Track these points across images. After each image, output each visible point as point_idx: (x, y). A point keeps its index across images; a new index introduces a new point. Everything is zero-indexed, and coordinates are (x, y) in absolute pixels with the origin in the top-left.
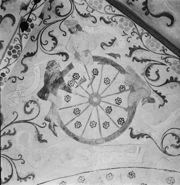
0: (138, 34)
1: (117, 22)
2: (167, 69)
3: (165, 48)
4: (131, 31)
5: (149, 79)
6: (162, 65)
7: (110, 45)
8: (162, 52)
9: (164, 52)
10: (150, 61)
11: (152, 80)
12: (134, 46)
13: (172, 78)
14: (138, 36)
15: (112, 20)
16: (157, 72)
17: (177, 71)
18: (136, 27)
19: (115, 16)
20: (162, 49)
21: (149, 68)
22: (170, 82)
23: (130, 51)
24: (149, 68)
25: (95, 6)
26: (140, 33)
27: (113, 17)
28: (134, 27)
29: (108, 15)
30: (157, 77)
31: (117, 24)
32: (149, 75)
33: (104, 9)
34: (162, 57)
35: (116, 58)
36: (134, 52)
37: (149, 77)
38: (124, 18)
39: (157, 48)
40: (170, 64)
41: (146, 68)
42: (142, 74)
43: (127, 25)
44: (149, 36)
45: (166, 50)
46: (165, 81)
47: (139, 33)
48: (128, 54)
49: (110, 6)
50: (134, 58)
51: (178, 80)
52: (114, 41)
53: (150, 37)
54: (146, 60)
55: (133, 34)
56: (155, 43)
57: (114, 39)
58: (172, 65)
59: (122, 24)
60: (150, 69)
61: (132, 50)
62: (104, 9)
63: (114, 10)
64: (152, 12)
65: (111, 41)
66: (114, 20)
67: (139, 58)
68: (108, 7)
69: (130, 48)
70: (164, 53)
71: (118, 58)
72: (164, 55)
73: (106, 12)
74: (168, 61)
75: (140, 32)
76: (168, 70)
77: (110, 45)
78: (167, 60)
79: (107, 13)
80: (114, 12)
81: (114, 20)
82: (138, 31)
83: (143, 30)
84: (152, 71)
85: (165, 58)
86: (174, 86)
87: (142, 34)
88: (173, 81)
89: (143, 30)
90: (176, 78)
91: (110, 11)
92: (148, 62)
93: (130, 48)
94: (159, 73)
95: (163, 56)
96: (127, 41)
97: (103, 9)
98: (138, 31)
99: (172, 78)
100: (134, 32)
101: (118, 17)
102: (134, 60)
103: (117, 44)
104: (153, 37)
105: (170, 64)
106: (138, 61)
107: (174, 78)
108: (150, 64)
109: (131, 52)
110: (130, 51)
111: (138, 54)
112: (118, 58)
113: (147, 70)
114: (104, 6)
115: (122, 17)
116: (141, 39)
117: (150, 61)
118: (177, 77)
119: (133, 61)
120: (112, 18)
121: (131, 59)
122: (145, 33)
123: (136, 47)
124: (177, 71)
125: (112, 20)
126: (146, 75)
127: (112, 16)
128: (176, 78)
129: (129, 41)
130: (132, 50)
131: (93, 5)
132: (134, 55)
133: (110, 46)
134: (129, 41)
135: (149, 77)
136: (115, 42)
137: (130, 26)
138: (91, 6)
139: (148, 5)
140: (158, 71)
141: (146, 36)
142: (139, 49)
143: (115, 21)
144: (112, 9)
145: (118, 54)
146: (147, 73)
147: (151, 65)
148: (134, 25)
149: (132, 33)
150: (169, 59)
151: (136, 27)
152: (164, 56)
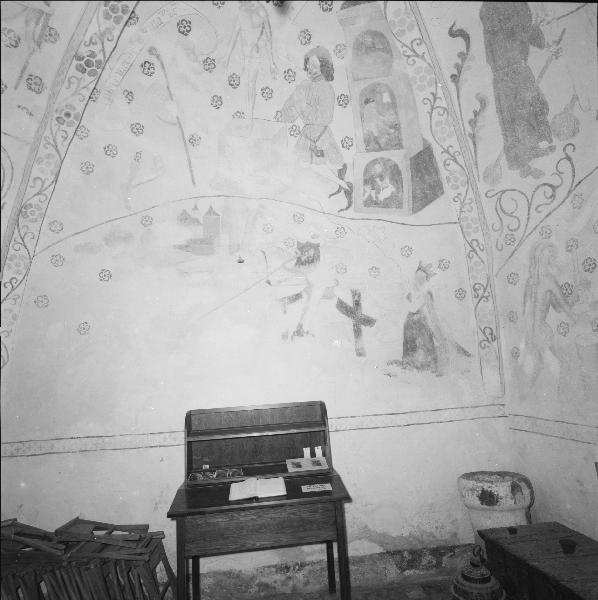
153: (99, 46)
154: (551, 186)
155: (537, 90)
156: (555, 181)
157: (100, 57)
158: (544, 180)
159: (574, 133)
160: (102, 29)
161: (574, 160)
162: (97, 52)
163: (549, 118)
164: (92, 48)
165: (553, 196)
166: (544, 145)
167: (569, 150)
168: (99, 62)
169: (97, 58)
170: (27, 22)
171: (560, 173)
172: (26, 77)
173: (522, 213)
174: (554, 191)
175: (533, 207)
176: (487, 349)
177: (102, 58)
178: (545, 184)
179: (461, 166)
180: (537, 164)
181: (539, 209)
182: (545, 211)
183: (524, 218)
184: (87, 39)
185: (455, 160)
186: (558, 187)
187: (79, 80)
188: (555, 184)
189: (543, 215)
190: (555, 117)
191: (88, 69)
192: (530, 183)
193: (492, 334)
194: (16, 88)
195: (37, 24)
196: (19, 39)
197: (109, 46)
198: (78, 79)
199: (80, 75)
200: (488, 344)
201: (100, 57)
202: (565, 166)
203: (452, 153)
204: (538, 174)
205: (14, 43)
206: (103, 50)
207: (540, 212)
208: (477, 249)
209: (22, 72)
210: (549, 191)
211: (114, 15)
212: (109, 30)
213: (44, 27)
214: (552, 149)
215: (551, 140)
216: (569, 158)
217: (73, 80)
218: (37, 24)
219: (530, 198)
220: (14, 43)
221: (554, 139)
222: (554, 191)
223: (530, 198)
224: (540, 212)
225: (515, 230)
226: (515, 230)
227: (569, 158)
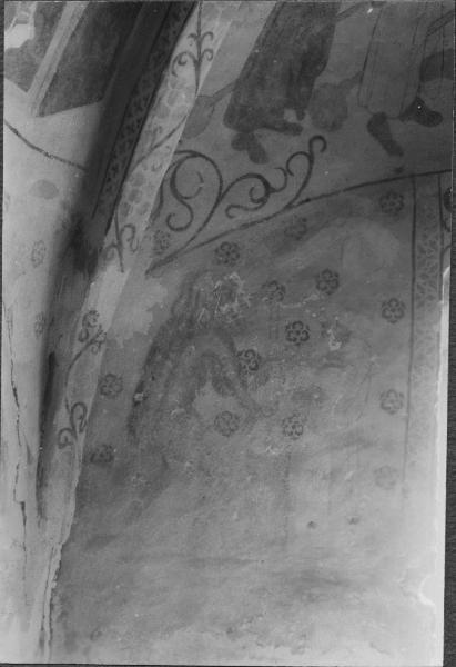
154: (266, 184)
155: (331, 28)
156: (275, 179)
158: (259, 169)
159: (334, 127)
161: (315, 166)
163: (319, 81)
165: (263, 201)
166: (290, 116)
167: (318, 145)
171: (287, 172)
173: (202, 206)
174: (267, 194)
175: (223, 205)
176: (68, 448)
178: (259, 177)
179: (197, 84)
180: (268, 140)
181: (232, 212)
182: (241, 216)
183: (201, 215)
185: (198, 64)
186: (274, 190)
188: (272, 184)
189: (233, 224)
190: (324, 86)
192: (244, 163)
193: (82, 418)
200: (70, 438)
202: (300, 164)
203: (204, 47)
204: (258, 155)
207: (231, 217)
208: (126, 244)
210: (260, 191)
214: (297, 130)
215: (303, 114)
216: (311, 158)
219: (225, 188)
221: (308, 117)
222: (267, 194)
223: (225, 188)
224: (231, 217)
225: (180, 229)
226: (180, 229)
227: (311, 158)
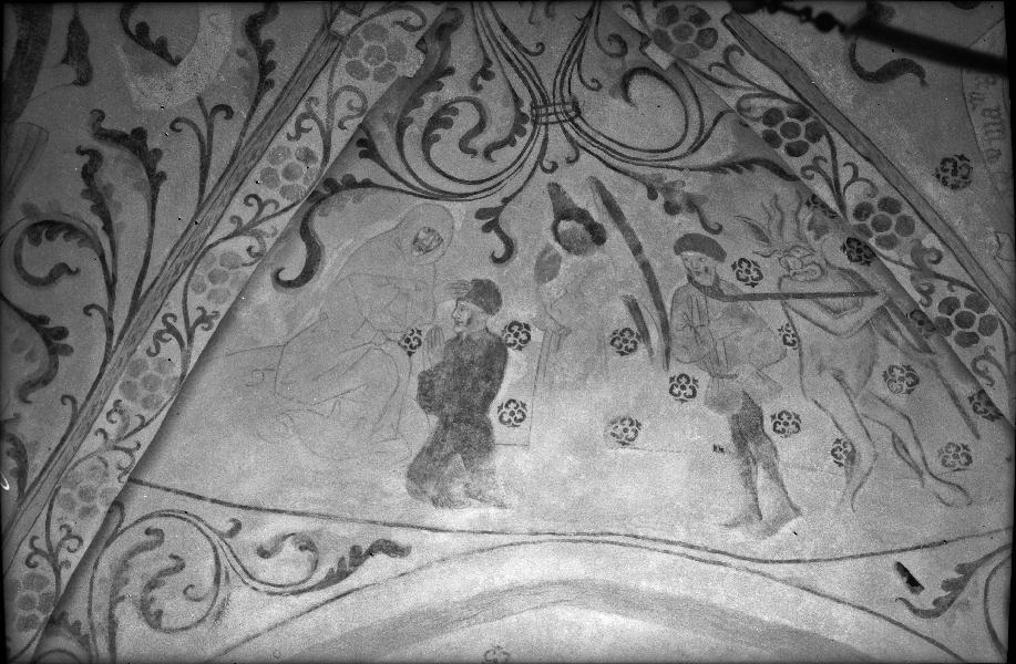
0: (257, 220)
1: (297, 137)
2: (93, 306)
3: (216, 322)
4: (265, 193)
5: (19, 244)
6: (107, 282)
7: (133, 29)
8: (194, 315)
9: (197, 323)
10: (108, 228)
11: (18, 261)
12: (157, 152)
13: (62, 333)
14: (245, 223)
15: (304, 116)
16: (63, 269)
17: (132, 379)
18: (286, 210)
19: (322, 131)
20: (209, 313)
21: (71, 230)
22: (38, 331)
23: (129, 133)
24: (71, 230)
25: (362, 52)
26: (260, 227)
27: (319, 123)
28: (285, 203)
29: (324, 99)
30: (42, 274)
31: (289, 138)
32: (36, 241)
33: (348, 88)
34: (172, 315)
35: (65, 61)
36: (127, 154)
37: (26, 243)
38: (318, 165)
39: (209, 297)
40: (153, 350)
41: (68, 220)
42: (29, 210)
43: (287, 178)
44: (253, 260)
45: (206, 326)
46: (35, 311)
47: (260, 222)
48: (106, 125)
49: (362, 111)
50: (95, 156)
51: (60, 357)
52: (161, 49)
53: (252, 264)
54: (102, 209)
55: (252, 200)
56: (227, 285)
57: (173, 50)
58: (150, 361)
59: (293, 159)
60: (66, 237)
61: (135, 142)
62: (348, 88)
63: (345, 124)
64: (317, 212)
65: (154, 37)
66: (306, 124)
67: (105, 176)
68: (358, 103)
69: (140, 134)
70: (191, 324)
71: (70, 73)
72: (187, 321)
73: (337, 94)
74: (165, 341)
75: (265, 227)
76: (91, 311)
77: (133, 29)
78: (167, 336)
79: (333, 99)
80: (341, 126)
81: (306, 124)
82: (269, 218)
83: (273, 235)
84: (64, 250)
85: (171, 329)
86: (26, 352)
87: (258, 236)
88: (48, 343)
89: (273, 235)
90: (67, 350)
91: (341, 110)
92: (97, 223)
93: (140, 134)
94: (65, 282)
95: (181, 319)
96: (177, 120)
97: (352, 81)
98: (269, 218)
99: (62, 333)
100: (262, 206)
101: (321, 142)
102: (86, 159)
103: (145, 70)
104: (250, 274)
105: (153, 350)
106: (87, 175)
107: (63, 342)
108: (91, 234)
109: (125, 136)
110: (129, 133)
111: (117, 171)
112: (70, 73)
113: (59, 223)
114: (362, 85)
115: (320, 158)
116: (235, 234)
117: (108, 228)
118: (72, 350)
119: (81, 152)
120: (315, 118)
121: (89, 142)
122: (263, 244)
123: (155, 163)
124: (132, 379)
125: (304, 116)
126: (35, 225)
127: (323, 117)
128: (67, 350)
129: (178, 126)
130: (135, 142)
131: (367, 45)
132: (109, 151)
133: (127, 31)
134: (178, 126)
135: (26, 243)
136: (153, 56)
137: (284, 192)
138: (359, 33)
139: (344, 194)
140: (70, 272)
141: (249, 250)
142: (150, 176)
143: (300, 130)
144: (352, 118)
145: (89, 70)
146: (48, 227)
147: (87, 237)
148: (293, 205)
149: (256, 197)
150: (174, 342)
151: (286, 210)
152: (180, 327)
153: (941, 286)
157: (962, 295)
160: (908, 260)
162: (948, 294)
164: (936, 300)
168: (970, 302)
169: (962, 300)
170: (892, 341)
172: (968, 407)
177: (968, 293)
184: (917, 297)
187: (986, 356)
191: (974, 329)
194: (978, 437)
195: (897, 329)
196: (908, 368)
197: (947, 267)
198: (983, 357)
199: (977, 349)
201: (962, 295)
205: (910, 380)
206: (952, 282)
209: (959, 407)
211: (892, 230)
212: (918, 251)
213: (905, 322)
217: (981, 365)
218: (897, 329)
220: (910, 380)
